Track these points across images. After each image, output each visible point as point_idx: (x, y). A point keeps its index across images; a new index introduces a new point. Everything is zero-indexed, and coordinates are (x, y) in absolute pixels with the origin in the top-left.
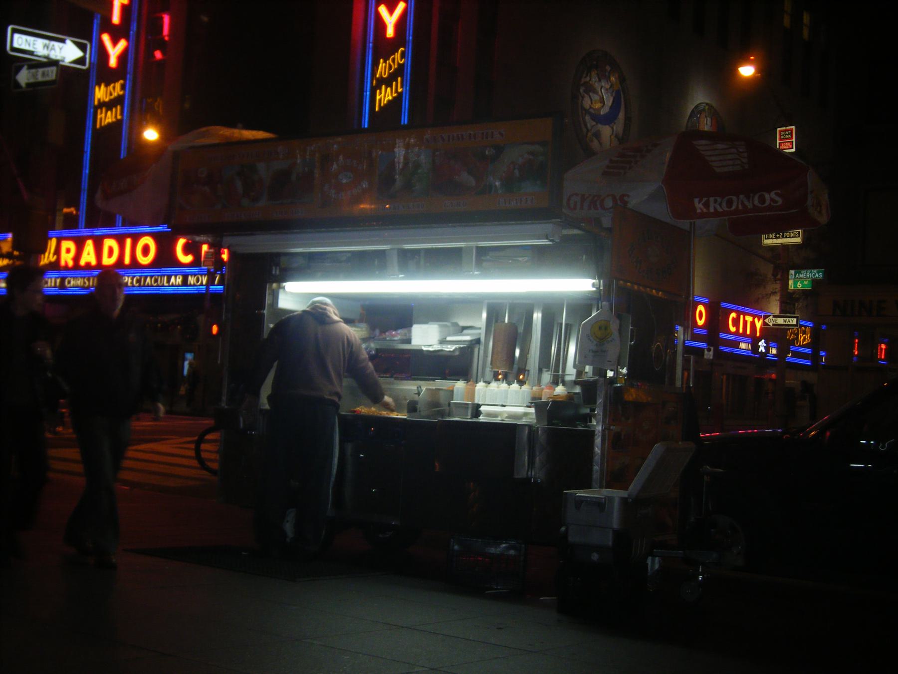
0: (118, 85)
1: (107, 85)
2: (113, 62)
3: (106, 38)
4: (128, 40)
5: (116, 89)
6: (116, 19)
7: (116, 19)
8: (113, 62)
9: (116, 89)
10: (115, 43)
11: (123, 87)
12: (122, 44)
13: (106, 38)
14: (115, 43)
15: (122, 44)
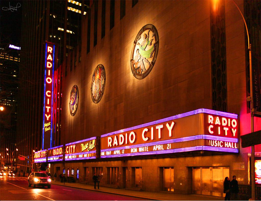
0: (49, 123)
1: (47, 123)
2: (48, 119)
3: (46, 115)
4: (51, 115)
5: (49, 124)
6: (48, 111)
7: (48, 111)
8: (48, 119)
9: (49, 124)
10: (48, 116)
11: (50, 123)
12: (50, 116)
13: (46, 115)
14: (48, 116)
15: (50, 116)
